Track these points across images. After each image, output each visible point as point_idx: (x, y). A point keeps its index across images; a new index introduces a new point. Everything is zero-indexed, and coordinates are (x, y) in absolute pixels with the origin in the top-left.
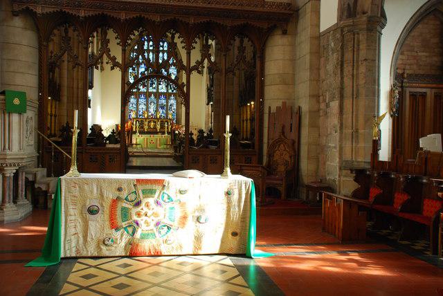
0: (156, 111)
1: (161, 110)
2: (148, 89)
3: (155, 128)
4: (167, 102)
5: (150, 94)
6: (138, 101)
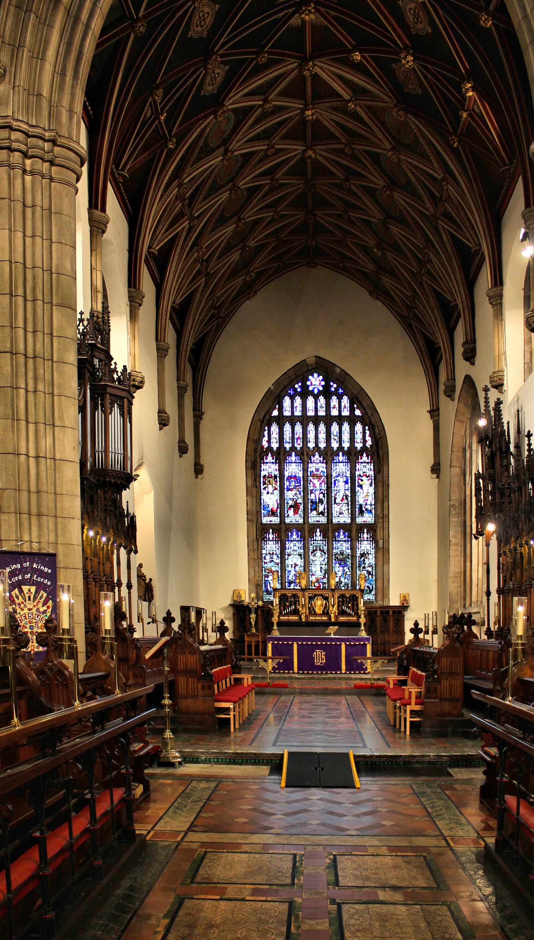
0: (328, 572)
1: (338, 569)
2: (306, 517)
3: (326, 612)
4: (353, 549)
5: (313, 528)
6: (283, 549)
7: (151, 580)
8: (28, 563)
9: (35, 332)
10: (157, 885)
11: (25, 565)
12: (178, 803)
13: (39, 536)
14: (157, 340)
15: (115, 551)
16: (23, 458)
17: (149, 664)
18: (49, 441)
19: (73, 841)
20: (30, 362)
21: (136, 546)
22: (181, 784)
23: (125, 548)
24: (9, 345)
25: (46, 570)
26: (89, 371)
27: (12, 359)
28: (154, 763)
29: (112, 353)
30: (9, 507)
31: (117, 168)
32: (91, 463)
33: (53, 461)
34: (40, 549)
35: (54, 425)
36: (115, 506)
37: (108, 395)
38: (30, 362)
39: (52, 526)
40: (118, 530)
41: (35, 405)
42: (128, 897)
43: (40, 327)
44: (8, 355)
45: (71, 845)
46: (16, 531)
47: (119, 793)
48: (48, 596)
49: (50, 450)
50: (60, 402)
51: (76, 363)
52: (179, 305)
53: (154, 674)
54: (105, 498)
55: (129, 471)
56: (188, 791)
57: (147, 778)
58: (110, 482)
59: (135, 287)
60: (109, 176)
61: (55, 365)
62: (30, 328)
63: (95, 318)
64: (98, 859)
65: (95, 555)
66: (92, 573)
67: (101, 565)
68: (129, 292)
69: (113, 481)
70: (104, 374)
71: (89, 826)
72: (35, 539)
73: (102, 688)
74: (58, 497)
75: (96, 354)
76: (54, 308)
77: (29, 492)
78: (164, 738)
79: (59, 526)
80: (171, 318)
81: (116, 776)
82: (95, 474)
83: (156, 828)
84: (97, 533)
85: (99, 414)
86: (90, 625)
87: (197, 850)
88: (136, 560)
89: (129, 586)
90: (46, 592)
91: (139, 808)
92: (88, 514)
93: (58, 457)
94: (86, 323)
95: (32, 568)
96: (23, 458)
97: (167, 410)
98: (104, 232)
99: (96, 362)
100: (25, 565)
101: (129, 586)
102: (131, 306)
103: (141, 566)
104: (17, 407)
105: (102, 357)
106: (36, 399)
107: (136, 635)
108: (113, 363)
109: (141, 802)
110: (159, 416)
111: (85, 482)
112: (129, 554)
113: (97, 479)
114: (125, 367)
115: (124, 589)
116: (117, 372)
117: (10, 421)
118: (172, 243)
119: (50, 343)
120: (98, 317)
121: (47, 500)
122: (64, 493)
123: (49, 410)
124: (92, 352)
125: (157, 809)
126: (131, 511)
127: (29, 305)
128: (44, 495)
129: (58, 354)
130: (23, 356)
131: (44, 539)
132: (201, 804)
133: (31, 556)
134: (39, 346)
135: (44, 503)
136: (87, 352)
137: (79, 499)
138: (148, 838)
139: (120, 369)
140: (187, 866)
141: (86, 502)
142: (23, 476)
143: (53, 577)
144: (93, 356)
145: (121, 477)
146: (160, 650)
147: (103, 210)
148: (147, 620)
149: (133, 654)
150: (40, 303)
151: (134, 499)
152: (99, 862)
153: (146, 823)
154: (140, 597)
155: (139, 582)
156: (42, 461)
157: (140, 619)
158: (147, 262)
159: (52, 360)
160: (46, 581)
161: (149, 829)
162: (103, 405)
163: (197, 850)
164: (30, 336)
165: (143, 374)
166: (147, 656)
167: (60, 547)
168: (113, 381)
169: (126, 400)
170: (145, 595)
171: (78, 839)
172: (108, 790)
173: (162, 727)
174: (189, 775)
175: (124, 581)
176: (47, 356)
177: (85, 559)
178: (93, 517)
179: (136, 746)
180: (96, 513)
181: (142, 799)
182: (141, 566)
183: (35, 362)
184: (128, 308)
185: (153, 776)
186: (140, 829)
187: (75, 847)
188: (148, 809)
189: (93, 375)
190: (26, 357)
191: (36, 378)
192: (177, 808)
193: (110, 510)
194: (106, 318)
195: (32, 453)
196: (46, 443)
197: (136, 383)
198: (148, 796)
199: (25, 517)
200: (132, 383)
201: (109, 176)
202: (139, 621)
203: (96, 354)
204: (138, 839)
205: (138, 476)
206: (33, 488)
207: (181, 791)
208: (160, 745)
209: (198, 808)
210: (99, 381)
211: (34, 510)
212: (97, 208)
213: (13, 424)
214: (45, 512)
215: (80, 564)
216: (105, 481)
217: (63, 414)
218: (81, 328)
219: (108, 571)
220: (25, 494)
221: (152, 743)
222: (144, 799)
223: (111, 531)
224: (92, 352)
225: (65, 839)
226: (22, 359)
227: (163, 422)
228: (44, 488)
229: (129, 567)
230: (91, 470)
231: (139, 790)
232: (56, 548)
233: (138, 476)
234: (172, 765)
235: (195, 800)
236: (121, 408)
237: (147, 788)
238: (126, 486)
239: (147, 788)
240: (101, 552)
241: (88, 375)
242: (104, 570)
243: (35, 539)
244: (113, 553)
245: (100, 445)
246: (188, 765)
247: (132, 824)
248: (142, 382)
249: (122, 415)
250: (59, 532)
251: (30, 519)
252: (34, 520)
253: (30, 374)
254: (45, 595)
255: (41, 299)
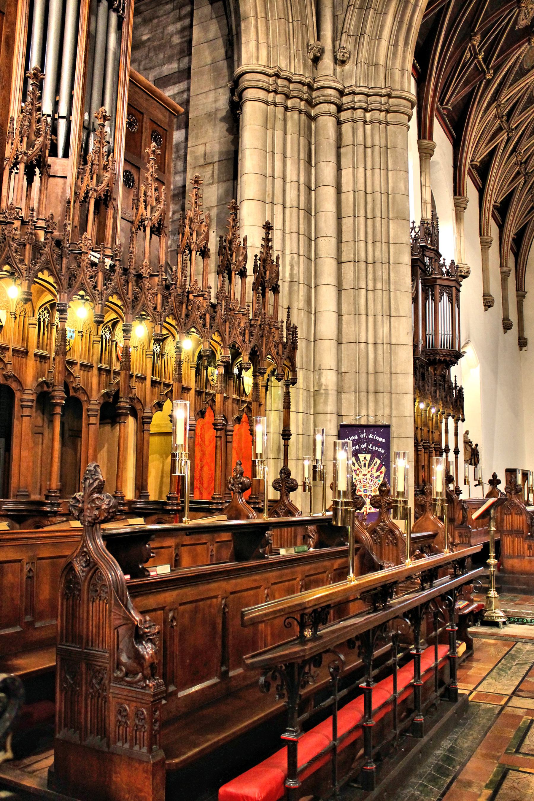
7: (477, 445)
8: (365, 435)
9: (374, 242)
10: (479, 750)
11: (362, 436)
12: (502, 664)
13: (376, 410)
14: (481, 235)
15: (444, 421)
16: (363, 346)
17: (475, 524)
18: (386, 329)
19: (397, 695)
20: (370, 267)
21: (463, 415)
22: (505, 645)
23: (453, 417)
24: (352, 256)
25: (381, 439)
26: (420, 268)
27: (355, 266)
28: (477, 622)
29: (441, 251)
30: (350, 387)
31: (442, 104)
32: (422, 347)
33: (389, 345)
34: (376, 422)
35: (390, 316)
36: (444, 381)
37: (438, 286)
38: (370, 267)
39: (387, 401)
40: (447, 402)
41: (374, 301)
42: (448, 759)
43: (378, 238)
44: (352, 263)
45: (395, 699)
46: (355, 408)
47: (443, 650)
48: (381, 462)
49: (387, 337)
50: (396, 296)
51: (410, 263)
52: (501, 203)
53: (479, 534)
54: (435, 374)
55: (457, 349)
56: (512, 652)
57: (470, 637)
58: (440, 360)
59: (460, 195)
60: (435, 112)
61: (391, 266)
62: (370, 240)
63: (425, 225)
64: (420, 715)
65: (426, 424)
66: (422, 441)
67: (430, 433)
68: (454, 199)
69: (443, 359)
70: (434, 269)
71: (412, 681)
72: (371, 413)
73: (429, 547)
74: (393, 375)
75: (427, 253)
76: (391, 221)
77: (368, 373)
78: (489, 597)
79: (393, 401)
80: (493, 216)
81: (441, 633)
82: (426, 354)
83: (478, 689)
84: (428, 405)
85: (430, 303)
86: (418, 488)
87: (522, 717)
88: (462, 427)
89: (456, 452)
90: (379, 459)
91: (461, 667)
92: (419, 389)
93: (393, 341)
94: (417, 230)
95: (368, 438)
96: (363, 346)
97: (491, 294)
98: (431, 156)
99: (427, 260)
100: (362, 436)
101: (456, 452)
102: (456, 211)
103: (467, 433)
104: (358, 304)
105: (432, 255)
106: (374, 296)
107: (462, 497)
108: (441, 259)
109: (464, 661)
110: (484, 300)
111: (417, 361)
112: (456, 422)
113: (427, 358)
114: (453, 262)
115: (451, 455)
116: (445, 266)
117: (353, 316)
118: (492, 154)
119: (387, 250)
120: (428, 224)
121: (384, 379)
122: (398, 372)
123: (386, 304)
124: (423, 252)
125: (480, 669)
126: (458, 384)
127: (370, 222)
128: (381, 376)
129: (394, 257)
130: (364, 263)
131: (380, 413)
132: (527, 668)
133: (367, 427)
134: (378, 253)
135: (380, 382)
136: (419, 253)
137: (412, 376)
138: (470, 698)
139: (448, 263)
140: (511, 733)
141: (418, 378)
142: (363, 361)
143: (387, 446)
144: (424, 256)
145: (450, 355)
146: (487, 512)
147: (431, 138)
148: (473, 483)
149: (459, 515)
150: (378, 219)
151: (461, 373)
152: (420, 719)
153: (468, 683)
154: (466, 461)
155: (465, 448)
156: (380, 346)
157: (466, 482)
158: (470, 174)
159: (389, 263)
160: (380, 450)
161: (472, 689)
162: (433, 295)
163: (522, 717)
164: (370, 247)
165: (469, 265)
166: (474, 516)
167: (394, 419)
168: (442, 273)
169: (454, 289)
170: (471, 459)
171: (401, 693)
172: (433, 647)
173: (487, 585)
174: (513, 636)
175: (452, 447)
176: (385, 260)
177: (416, 429)
178: (424, 391)
179: (460, 604)
180: (427, 388)
181: (464, 657)
182: (467, 433)
183: (374, 267)
184: (454, 212)
185: (475, 634)
186: (462, 689)
187: (399, 701)
188: (470, 668)
189: (424, 271)
190: (367, 263)
191: (375, 280)
192: (501, 670)
193: (440, 385)
194: (435, 223)
195: (371, 340)
196: (383, 331)
197: (463, 274)
198: (471, 655)
199: (363, 395)
200: (459, 274)
201: (435, 112)
202: (465, 484)
203: (427, 253)
204: (460, 699)
205: (465, 352)
206: (371, 369)
207: (505, 652)
208: (485, 604)
209: (523, 672)
210: (430, 276)
211: (371, 388)
212: (424, 138)
213: (355, 319)
214: (381, 389)
215: (412, 435)
216: (435, 359)
217: (398, 306)
218: (413, 234)
219: (436, 438)
220: (364, 375)
221: (476, 601)
222: (467, 657)
223: (441, 402)
224: (423, 252)
225: (389, 692)
226: (363, 265)
227: (488, 304)
228: (380, 369)
229: (456, 435)
230: (422, 351)
231: (462, 648)
232: (391, 420)
233: (465, 352)
234: (496, 624)
235: (520, 662)
236: (450, 296)
237: (469, 647)
238: (454, 363)
239: (469, 647)
240: (430, 422)
241: (419, 272)
242: (433, 438)
243: (371, 413)
244: (441, 423)
245: (430, 329)
246: (512, 625)
247: (455, 683)
248: (468, 272)
249: (451, 301)
250: (393, 406)
251: (368, 395)
252: (371, 397)
253: (370, 276)
254: (379, 462)
255: (379, 215)
